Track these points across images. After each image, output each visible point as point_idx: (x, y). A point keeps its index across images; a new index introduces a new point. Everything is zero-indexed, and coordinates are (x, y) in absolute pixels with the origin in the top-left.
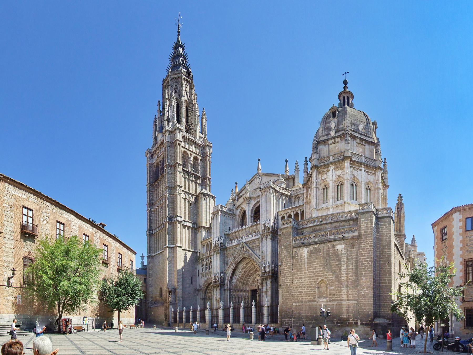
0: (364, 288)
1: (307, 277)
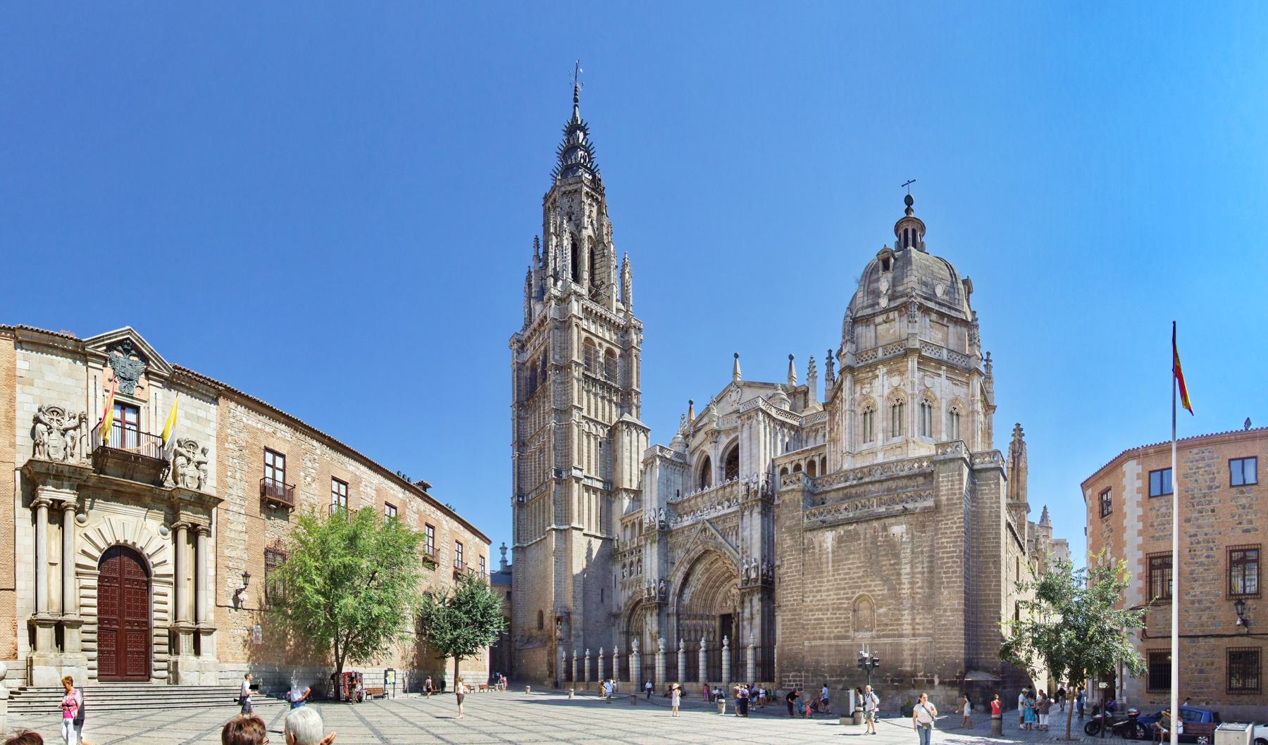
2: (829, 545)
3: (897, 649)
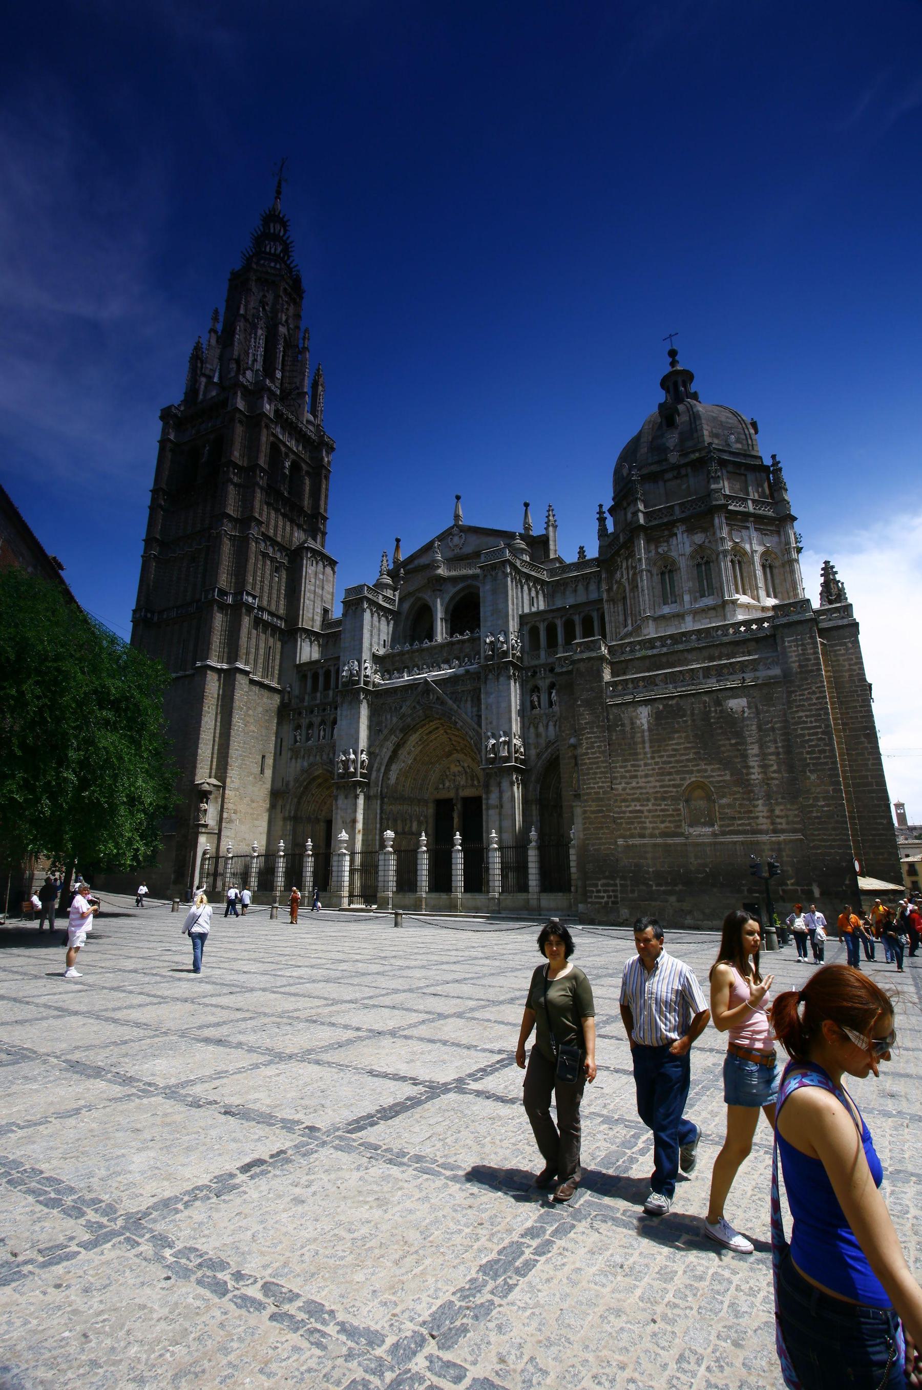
0: (816, 799)
1: (652, 776)
2: (644, 721)
3: (754, 846)
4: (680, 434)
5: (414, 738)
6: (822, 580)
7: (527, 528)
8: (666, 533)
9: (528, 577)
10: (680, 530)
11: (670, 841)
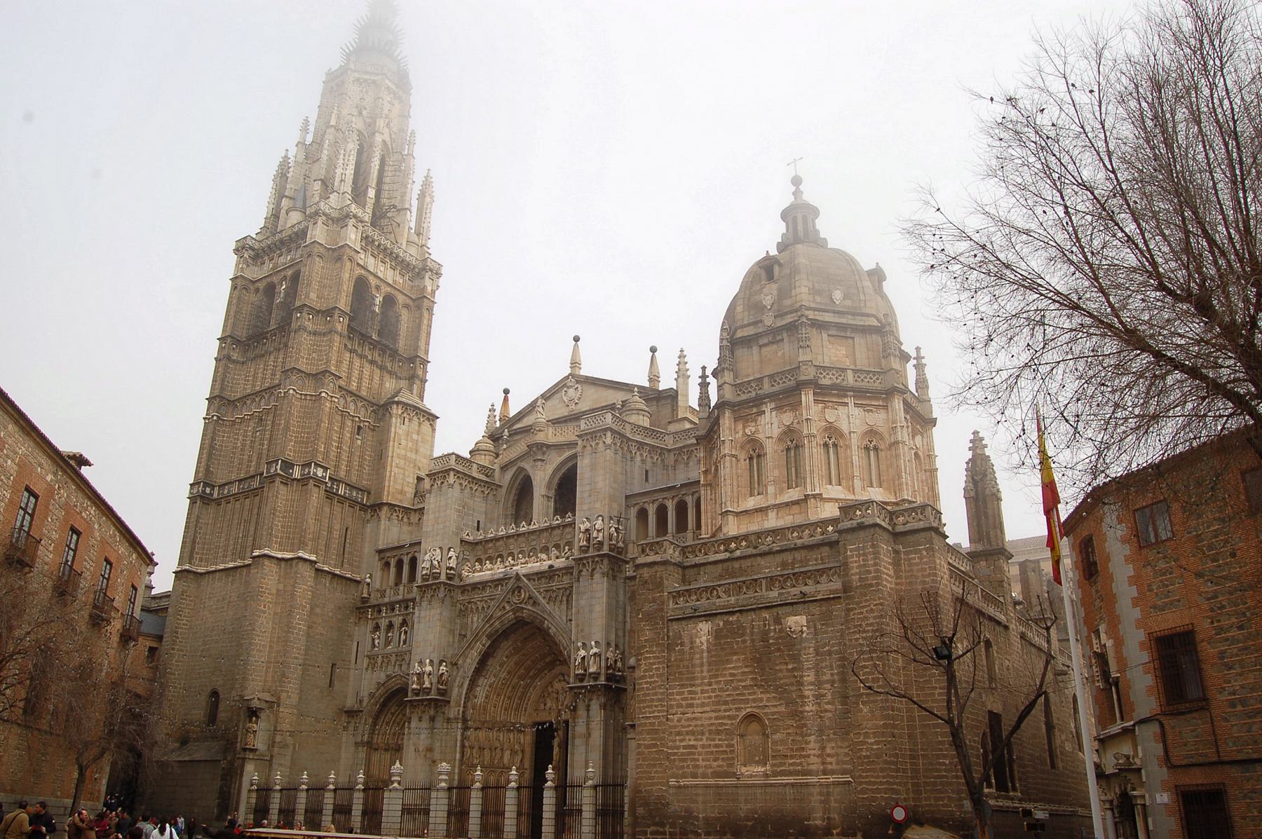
0: (867, 735)
1: (708, 704)
2: (704, 638)
4: (779, 290)
5: (506, 647)
6: (969, 455)
7: (654, 378)
8: (755, 410)
9: (641, 445)
10: (768, 407)
11: (721, 782)
